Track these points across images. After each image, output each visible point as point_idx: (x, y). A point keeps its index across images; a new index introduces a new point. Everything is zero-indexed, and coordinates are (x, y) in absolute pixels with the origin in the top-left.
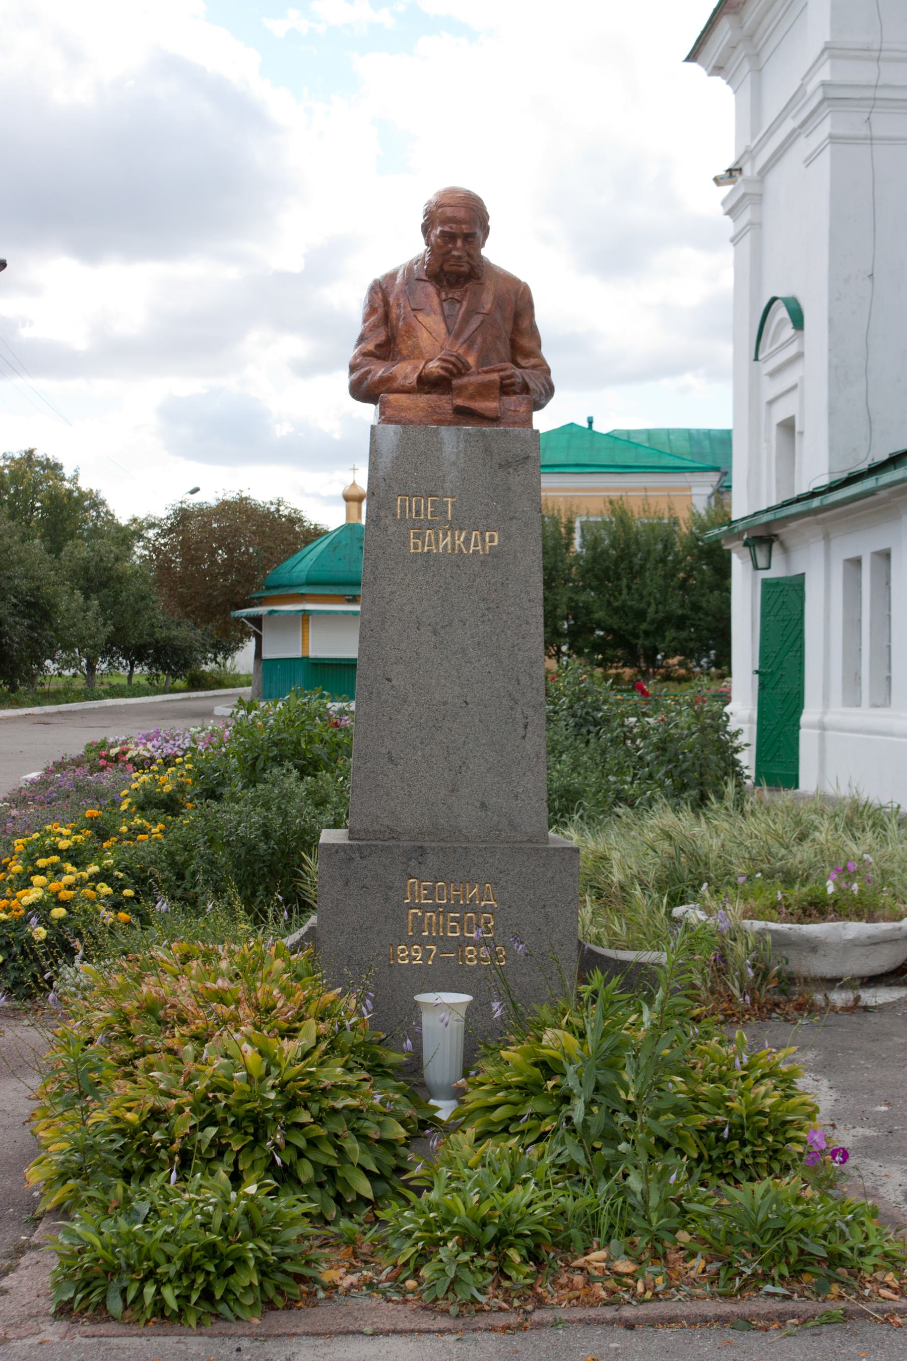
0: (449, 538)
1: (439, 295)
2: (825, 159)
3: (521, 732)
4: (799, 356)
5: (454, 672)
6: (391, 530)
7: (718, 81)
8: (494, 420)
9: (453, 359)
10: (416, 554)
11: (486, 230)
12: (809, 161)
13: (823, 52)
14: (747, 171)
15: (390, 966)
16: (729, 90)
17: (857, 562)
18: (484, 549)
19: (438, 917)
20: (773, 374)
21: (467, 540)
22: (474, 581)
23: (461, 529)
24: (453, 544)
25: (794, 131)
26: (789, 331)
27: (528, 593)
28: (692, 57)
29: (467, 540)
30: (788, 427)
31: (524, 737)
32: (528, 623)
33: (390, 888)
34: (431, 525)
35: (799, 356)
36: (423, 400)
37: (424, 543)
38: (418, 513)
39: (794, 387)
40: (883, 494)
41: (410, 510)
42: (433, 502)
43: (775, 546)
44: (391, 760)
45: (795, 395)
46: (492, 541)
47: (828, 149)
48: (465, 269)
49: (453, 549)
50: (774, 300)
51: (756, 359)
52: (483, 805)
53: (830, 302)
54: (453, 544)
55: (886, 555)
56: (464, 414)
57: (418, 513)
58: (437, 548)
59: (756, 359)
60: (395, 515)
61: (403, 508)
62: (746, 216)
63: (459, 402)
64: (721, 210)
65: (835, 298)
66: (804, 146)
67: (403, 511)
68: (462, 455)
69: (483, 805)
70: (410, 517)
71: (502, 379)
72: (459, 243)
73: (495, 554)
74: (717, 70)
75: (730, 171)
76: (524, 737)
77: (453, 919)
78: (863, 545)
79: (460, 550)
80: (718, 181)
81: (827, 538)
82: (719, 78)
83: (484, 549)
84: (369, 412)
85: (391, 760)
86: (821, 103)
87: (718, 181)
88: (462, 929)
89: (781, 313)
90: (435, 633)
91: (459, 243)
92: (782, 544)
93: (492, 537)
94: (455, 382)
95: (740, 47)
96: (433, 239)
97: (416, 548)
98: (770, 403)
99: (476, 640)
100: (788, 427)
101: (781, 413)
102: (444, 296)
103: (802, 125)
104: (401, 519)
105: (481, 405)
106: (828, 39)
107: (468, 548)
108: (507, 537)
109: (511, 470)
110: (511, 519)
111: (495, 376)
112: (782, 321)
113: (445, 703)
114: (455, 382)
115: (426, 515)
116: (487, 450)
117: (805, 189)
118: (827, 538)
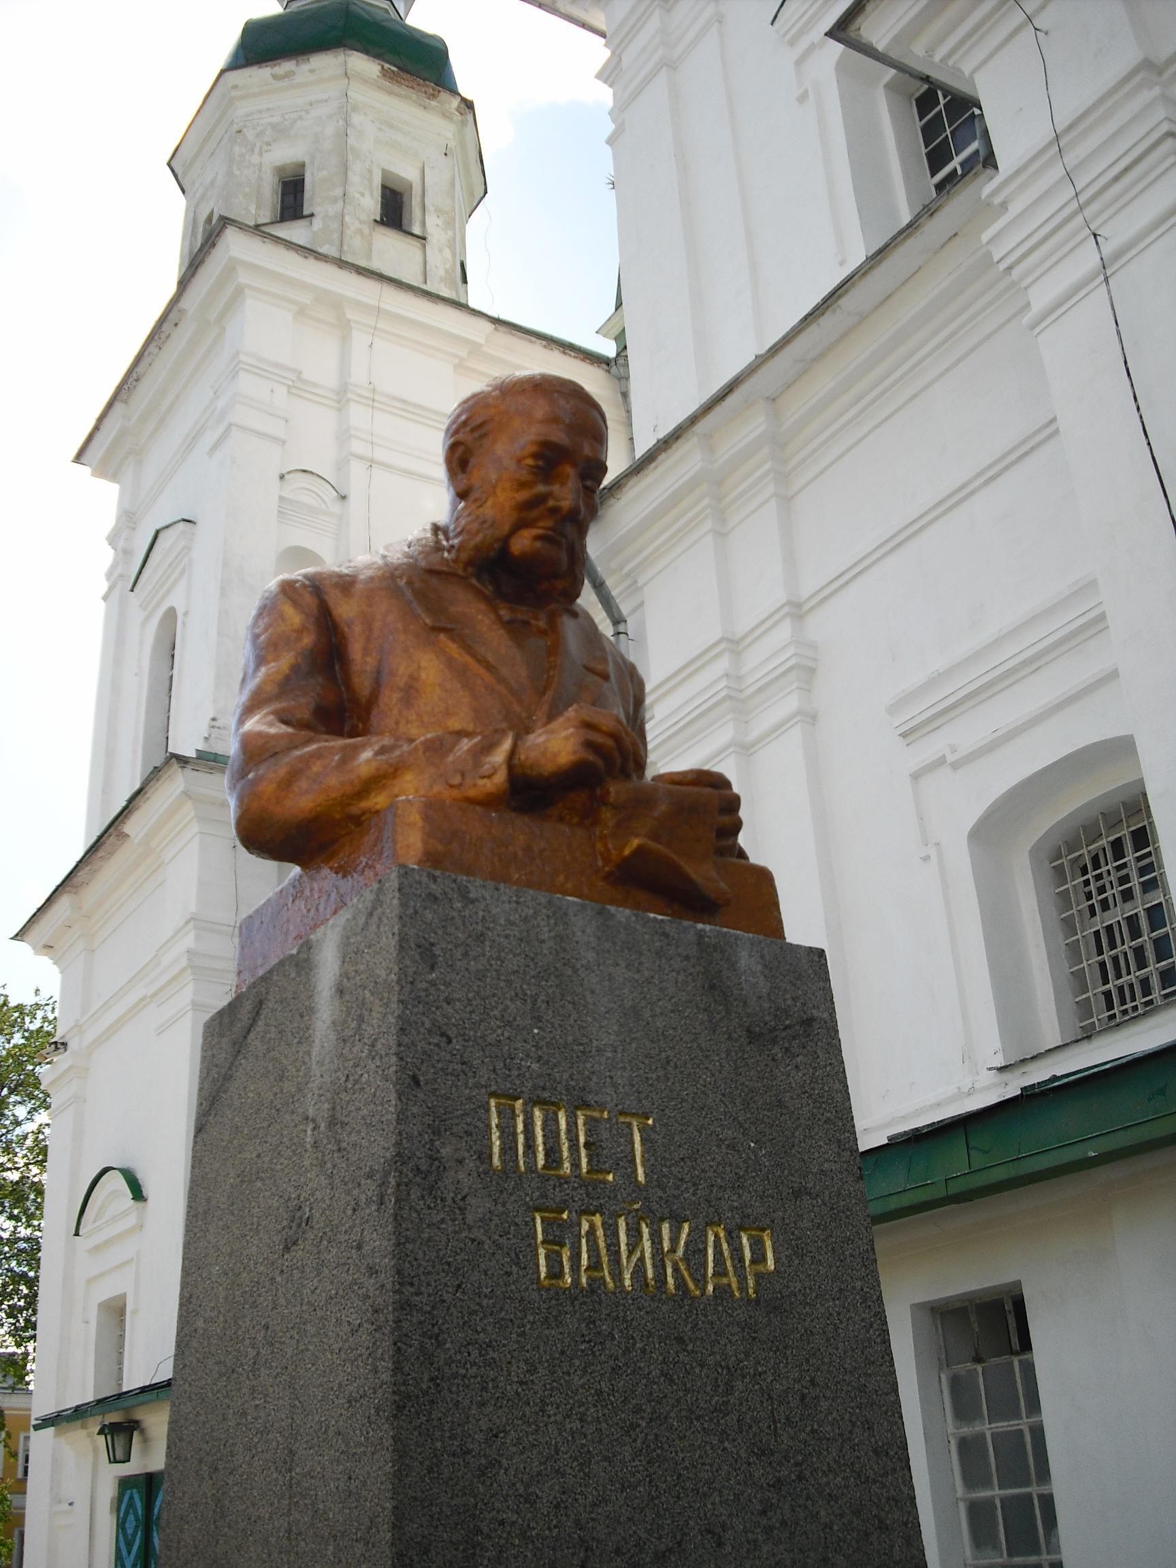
0: (647, 1244)
6: (478, 1206)
7: (45, 962)
10: (559, 1292)
12: (161, 1030)
13: (187, 922)
16: (56, 969)
18: (743, 1288)
21: (696, 1251)
22: (729, 1390)
24: (660, 1266)
28: (19, 936)
29: (696, 1251)
34: (592, 1196)
36: (521, 831)
37: (575, 1257)
41: (530, 1146)
42: (591, 1124)
43: (136, 1437)
46: (759, 1258)
51: (77, 1234)
57: (552, 1153)
58: (617, 1276)
59: (77, 1234)
60: (484, 1156)
67: (509, 1148)
73: (772, 1300)
82: (46, 958)
83: (743, 1288)
89: (115, 1184)
92: (142, 1432)
93: (757, 1245)
97: (555, 1273)
101: (106, 1291)
103: (155, 994)
107: (701, 1281)
108: (792, 1250)
110: (797, 1194)
115: (576, 1165)
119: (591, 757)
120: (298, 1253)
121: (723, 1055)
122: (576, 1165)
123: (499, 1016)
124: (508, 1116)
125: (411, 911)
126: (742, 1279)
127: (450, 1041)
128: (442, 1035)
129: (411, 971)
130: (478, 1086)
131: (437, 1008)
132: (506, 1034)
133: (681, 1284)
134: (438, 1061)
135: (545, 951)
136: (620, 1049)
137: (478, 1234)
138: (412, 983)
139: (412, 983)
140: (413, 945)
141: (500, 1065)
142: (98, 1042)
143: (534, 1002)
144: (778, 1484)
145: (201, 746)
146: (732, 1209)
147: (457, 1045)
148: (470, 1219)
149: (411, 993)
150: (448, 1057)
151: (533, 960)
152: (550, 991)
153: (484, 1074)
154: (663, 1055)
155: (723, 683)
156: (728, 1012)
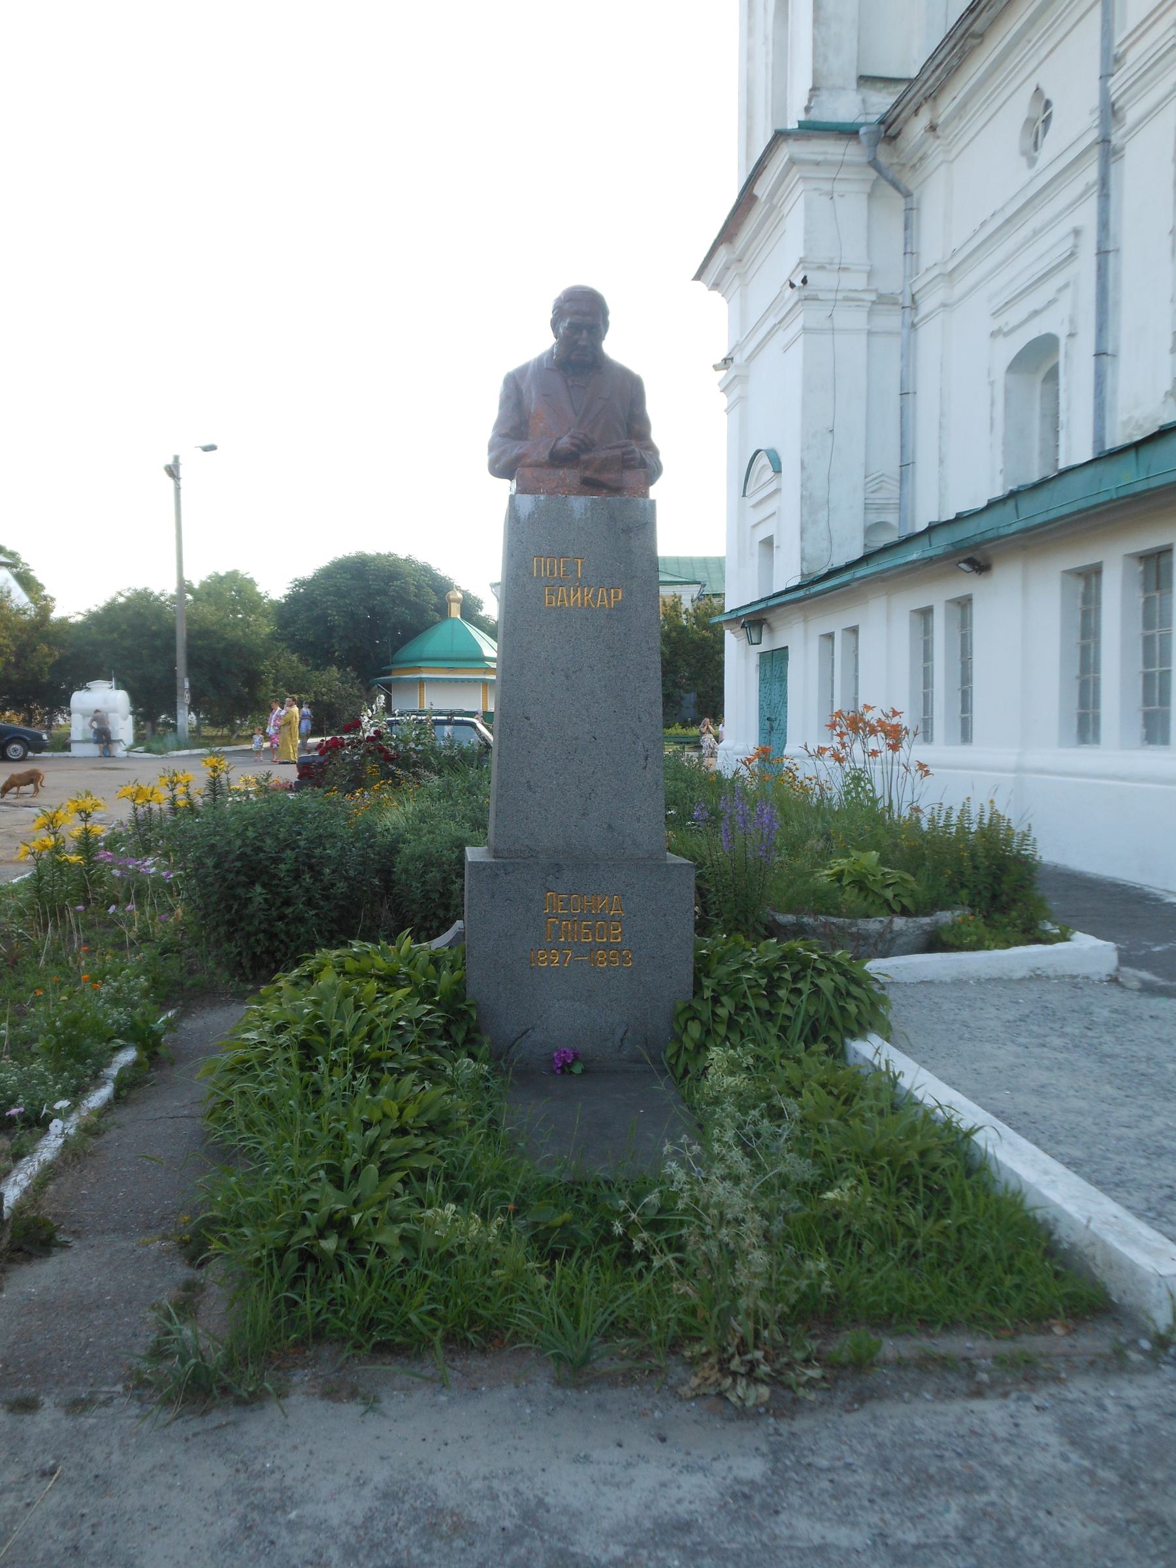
1: (566, 382)
2: (798, 349)
3: (642, 762)
4: (777, 491)
5: (584, 712)
7: (716, 294)
8: (617, 490)
9: (581, 436)
11: (606, 324)
12: (786, 349)
14: (738, 359)
15: (532, 968)
17: (830, 636)
18: (609, 603)
19: (573, 924)
20: (755, 506)
21: (595, 595)
23: (590, 587)
24: (583, 599)
25: (775, 325)
26: (769, 473)
27: (647, 642)
28: (698, 277)
29: (595, 595)
30: (768, 543)
31: (645, 768)
32: (647, 668)
33: (531, 900)
35: (777, 491)
38: (552, 573)
39: (774, 514)
40: (854, 585)
44: (530, 787)
45: (774, 518)
47: (801, 339)
49: (582, 604)
50: (758, 452)
51: (744, 495)
52: (610, 826)
53: (802, 450)
54: (583, 599)
55: (854, 630)
56: (590, 485)
57: (552, 573)
61: (539, 567)
62: (736, 392)
63: (588, 474)
64: (718, 389)
65: (806, 448)
66: (781, 338)
67: (539, 571)
69: (610, 826)
71: (624, 454)
72: (585, 334)
74: (715, 286)
75: (725, 360)
76: (645, 768)
77: (586, 927)
78: (836, 622)
79: (589, 605)
80: (716, 368)
81: (806, 620)
84: (506, 487)
85: (530, 787)
86: (796, 304)
87: (716, 368)
88: (594, 936)
89: (763, 460)
90: (567, 677)
91: (585, 334)
94: (584, 457)
95: (733, 267)
96: (561, 331)
98: (754, 526)
99: (603, 683)
100: (768, 543)
101: (762, 534)
102: (570, 383)
103: (780, 322)
104: (537, 577)
105: (606, 477)
106: (802, 255)
107: (596, 604)
110: (633, 577)
111: (618, 452)
112: (764, 466)
113: (576, 739)
114: (584, 457)
115: (559, 573)
117: (783, 369)
118: (806, 620)
119: (573, 449)
122: (559, 573)
124: (539, 562)
126: (609, 603)
133: (589, 605)
142: (751, 358)
144: (613, 656)
145: (802, 117)
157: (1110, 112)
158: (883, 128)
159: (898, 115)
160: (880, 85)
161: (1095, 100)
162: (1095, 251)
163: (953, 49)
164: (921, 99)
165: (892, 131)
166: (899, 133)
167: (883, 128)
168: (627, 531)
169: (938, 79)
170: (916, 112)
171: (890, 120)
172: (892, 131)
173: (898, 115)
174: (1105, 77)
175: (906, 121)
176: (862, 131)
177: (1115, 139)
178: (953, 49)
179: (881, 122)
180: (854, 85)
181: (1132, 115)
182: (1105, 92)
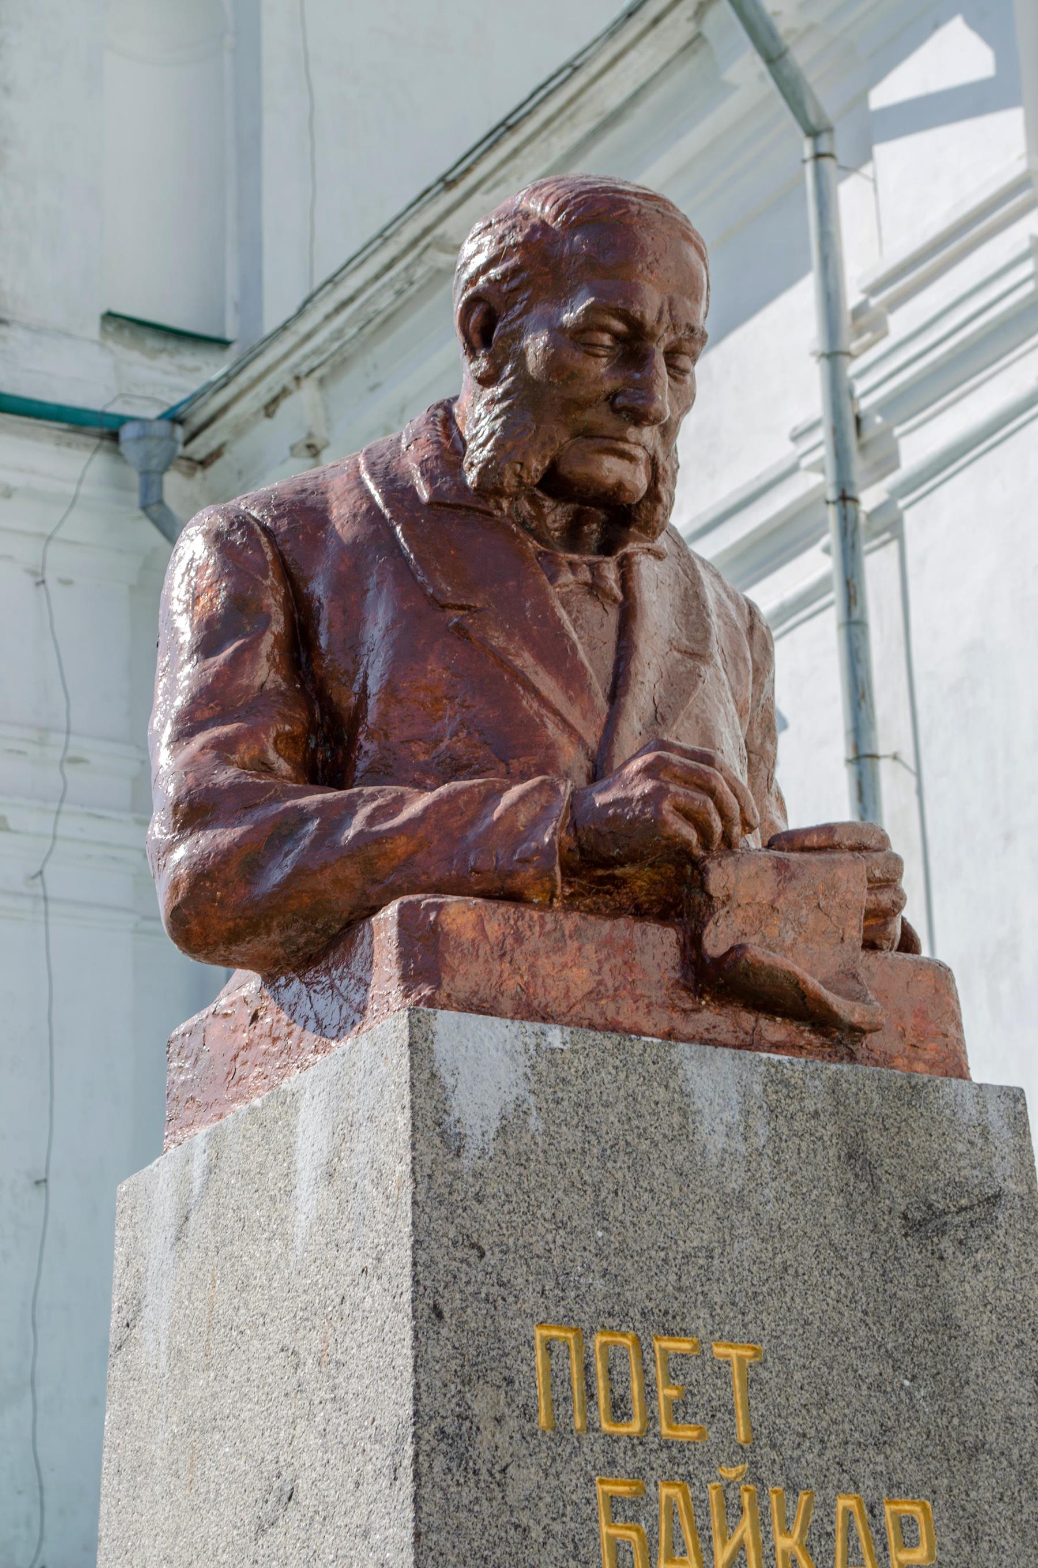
6: (525, 1478)
48: (639, 480)
60: (527, 1413)
68: (766, 1164)
70: (591, 1427)
104: (560, 1432)
109: (946, 1244)
116: (854, 1155)
120: (276, 1536)
121: (866, 1255)
123: (548, 1216)
125: (425, 1076)
127: (482, 1255)
128: (473, 1246)
129: (427, 1160)
130: (521, 1313)
131: (465, 1209)
132: (559, 1242)
134: (468, 1283)
135: (612, 1118)
136: (718, 1251)
137: (525, 1519)
138: (430, 1176)
139: (430, 1176)
140: (429, 1123)
141: (549, 1285)
143: (597, 1191)
146: (874, 1474)
147: (492, 1259)
148: (511, 1499)
149: (429, 1189)
150: (480, 1277)
151: (594, 1132)
152: (619, 1175)
153: (531, 1299)
154: (779, 1259)
155: (1027, 268)
156: (875, 1188)
157: (852, 435)
158: (180, 433)
159: (224, 409)
160: (152, 342)
161: (811, 403)
162: (840, 749)
163: (389, 267)
164: (287, 380)
165: (200, 448)
166: (216, 454)
167: (180, 433)
168: (924, 1223)
169: (339, 333)
170: (270, 408)
171: (198, 420)
172: (200, 448)
173: (224, 409)
174: (834, 356)
175: (239, 431)
176: (128, 432)
177: (870, 499)
178: (389, 267)
179: (174, 418)
180: (93, 328)
181: (918, 445)
182: (838, 391)
